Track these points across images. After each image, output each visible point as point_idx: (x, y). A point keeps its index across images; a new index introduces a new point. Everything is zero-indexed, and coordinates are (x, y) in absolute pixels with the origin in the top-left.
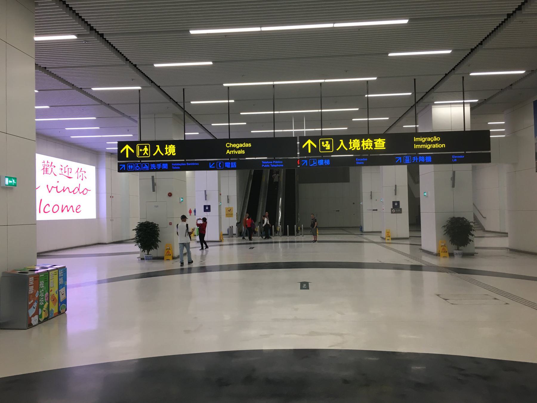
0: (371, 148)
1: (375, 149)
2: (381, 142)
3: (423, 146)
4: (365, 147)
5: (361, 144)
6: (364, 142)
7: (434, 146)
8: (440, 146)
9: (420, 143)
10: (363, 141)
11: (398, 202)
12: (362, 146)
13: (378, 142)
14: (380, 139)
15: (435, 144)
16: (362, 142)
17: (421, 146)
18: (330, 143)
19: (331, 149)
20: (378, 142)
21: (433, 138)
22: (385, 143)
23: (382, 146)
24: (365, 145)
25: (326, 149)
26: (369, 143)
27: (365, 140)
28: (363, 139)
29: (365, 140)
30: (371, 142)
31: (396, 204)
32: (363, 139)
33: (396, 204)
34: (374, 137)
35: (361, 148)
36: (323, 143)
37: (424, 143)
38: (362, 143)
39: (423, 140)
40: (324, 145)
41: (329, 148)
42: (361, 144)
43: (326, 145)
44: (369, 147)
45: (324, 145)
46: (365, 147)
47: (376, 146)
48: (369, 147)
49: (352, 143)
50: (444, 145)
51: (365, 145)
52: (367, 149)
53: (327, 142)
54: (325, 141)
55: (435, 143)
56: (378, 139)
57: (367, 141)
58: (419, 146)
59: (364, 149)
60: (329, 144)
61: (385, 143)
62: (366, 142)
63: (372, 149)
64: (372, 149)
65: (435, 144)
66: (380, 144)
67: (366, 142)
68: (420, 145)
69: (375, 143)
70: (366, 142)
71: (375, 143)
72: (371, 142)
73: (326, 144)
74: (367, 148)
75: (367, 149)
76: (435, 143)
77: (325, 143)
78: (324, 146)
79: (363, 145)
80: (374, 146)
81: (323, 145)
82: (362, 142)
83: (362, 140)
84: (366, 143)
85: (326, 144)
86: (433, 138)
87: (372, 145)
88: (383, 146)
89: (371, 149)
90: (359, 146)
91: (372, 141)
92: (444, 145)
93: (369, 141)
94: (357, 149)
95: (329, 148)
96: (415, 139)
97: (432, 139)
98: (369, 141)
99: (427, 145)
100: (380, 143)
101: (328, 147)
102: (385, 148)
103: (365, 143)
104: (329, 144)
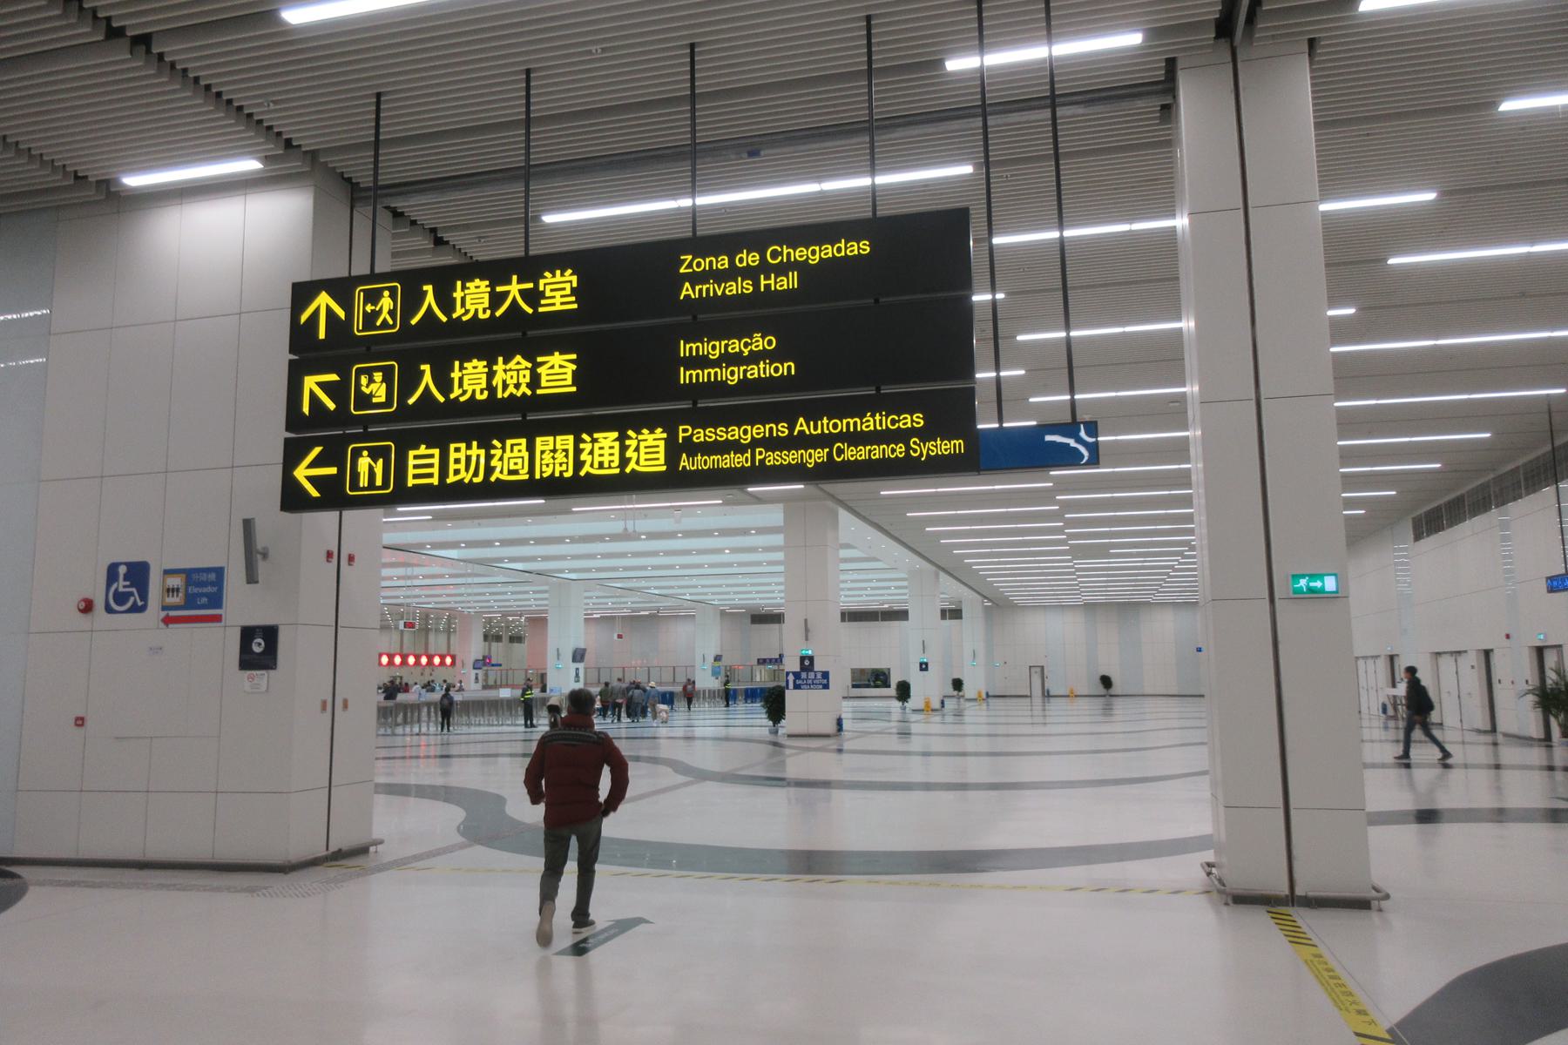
0: (524, 389)
1: (539, 392)
2: (561, 366)
3: (712, 371)
4: (505, 386)
5: (491, 375)
6: (504, 367)
7: (754, 372)
8: (776, 370)
9: (701, 362)
10: (499, 367)
11: (811, 659)
12: (494, 383)
13: (552, 367)
14: (557, 354)
15: (758, 364)
16: (495, 368)
17: (704, 375)
18: (388, 379)
19: (388, 403)
20: (552, 367)
21: (751, 338)
22: (574, 367)
23: (565, 380)
24: (504, 382)
25: (375, 400)
26: (518, 370)
27: (505, 362)
28: (500, 359)
29: (505, 362)
30: (526, 368)
31: (807, 663)
32: (500, 359)
33: (807, 663)
34: (533, 349)
35: (491, 389)
36: (364, 380)
37: (715, 364)
38: (495, 372)
39: (713, 349)
40: (367, 386)
41: (383, 399)
42: (491, 375)
43: (373, 387)
44: (517, 386)
45: (367, 386)
46: (505, 386)
47: (544, 384)
48: (517, 386)
49: (460, 375)
50: (789, 367)
51: (504, 382)
52: (511, 394)
53: (378, 376)
54: (369, 372)
55: (755, 358)
56: (552, 354)
57: (512, 365)
58: (698, 375)
59: (500, 396)
60: (382, 382)
61: (574, 367)
62: (508, 367)
63: (529, 393)
64: (529, 393)
65: (758, 364)
66: (558, 372)
67: (510, 370)
68: (700, 372)
69: (539, 370)
70: (510, 370)
71: (539, 370)
72: (526, 368)
73: (374, 382)
74: (511, 389)
75: (511, 394)
76: (755, 358)
77: (371, 381)
78: (367, 391)
79: (498, 381)
80: (535, 382)
81: (364, 389)
82: (495, 368)
83: (496, 363)
84: (509, 373)
85: (374, 382)
86: (751, 338)
87: (528, 379)
88: (569, 382)
89: (524, 394)
90: (484, 386)
91: (529, 365)
92: (789, 367)
93: (518, 363)
94: (479, 397)
95: (383, 399)
96: (685, 349)
97: (746, 345)
98: (518, 363)
99: (727, 368)
100: (557, 370)
101: (377, 390)
102: (574, 389)
103: (505, 371)
104: (384, 384)
